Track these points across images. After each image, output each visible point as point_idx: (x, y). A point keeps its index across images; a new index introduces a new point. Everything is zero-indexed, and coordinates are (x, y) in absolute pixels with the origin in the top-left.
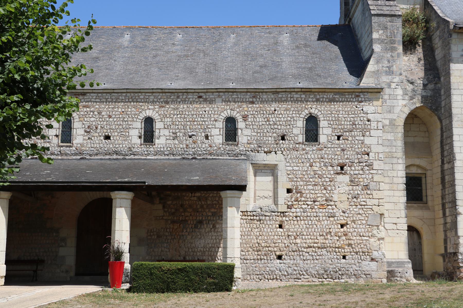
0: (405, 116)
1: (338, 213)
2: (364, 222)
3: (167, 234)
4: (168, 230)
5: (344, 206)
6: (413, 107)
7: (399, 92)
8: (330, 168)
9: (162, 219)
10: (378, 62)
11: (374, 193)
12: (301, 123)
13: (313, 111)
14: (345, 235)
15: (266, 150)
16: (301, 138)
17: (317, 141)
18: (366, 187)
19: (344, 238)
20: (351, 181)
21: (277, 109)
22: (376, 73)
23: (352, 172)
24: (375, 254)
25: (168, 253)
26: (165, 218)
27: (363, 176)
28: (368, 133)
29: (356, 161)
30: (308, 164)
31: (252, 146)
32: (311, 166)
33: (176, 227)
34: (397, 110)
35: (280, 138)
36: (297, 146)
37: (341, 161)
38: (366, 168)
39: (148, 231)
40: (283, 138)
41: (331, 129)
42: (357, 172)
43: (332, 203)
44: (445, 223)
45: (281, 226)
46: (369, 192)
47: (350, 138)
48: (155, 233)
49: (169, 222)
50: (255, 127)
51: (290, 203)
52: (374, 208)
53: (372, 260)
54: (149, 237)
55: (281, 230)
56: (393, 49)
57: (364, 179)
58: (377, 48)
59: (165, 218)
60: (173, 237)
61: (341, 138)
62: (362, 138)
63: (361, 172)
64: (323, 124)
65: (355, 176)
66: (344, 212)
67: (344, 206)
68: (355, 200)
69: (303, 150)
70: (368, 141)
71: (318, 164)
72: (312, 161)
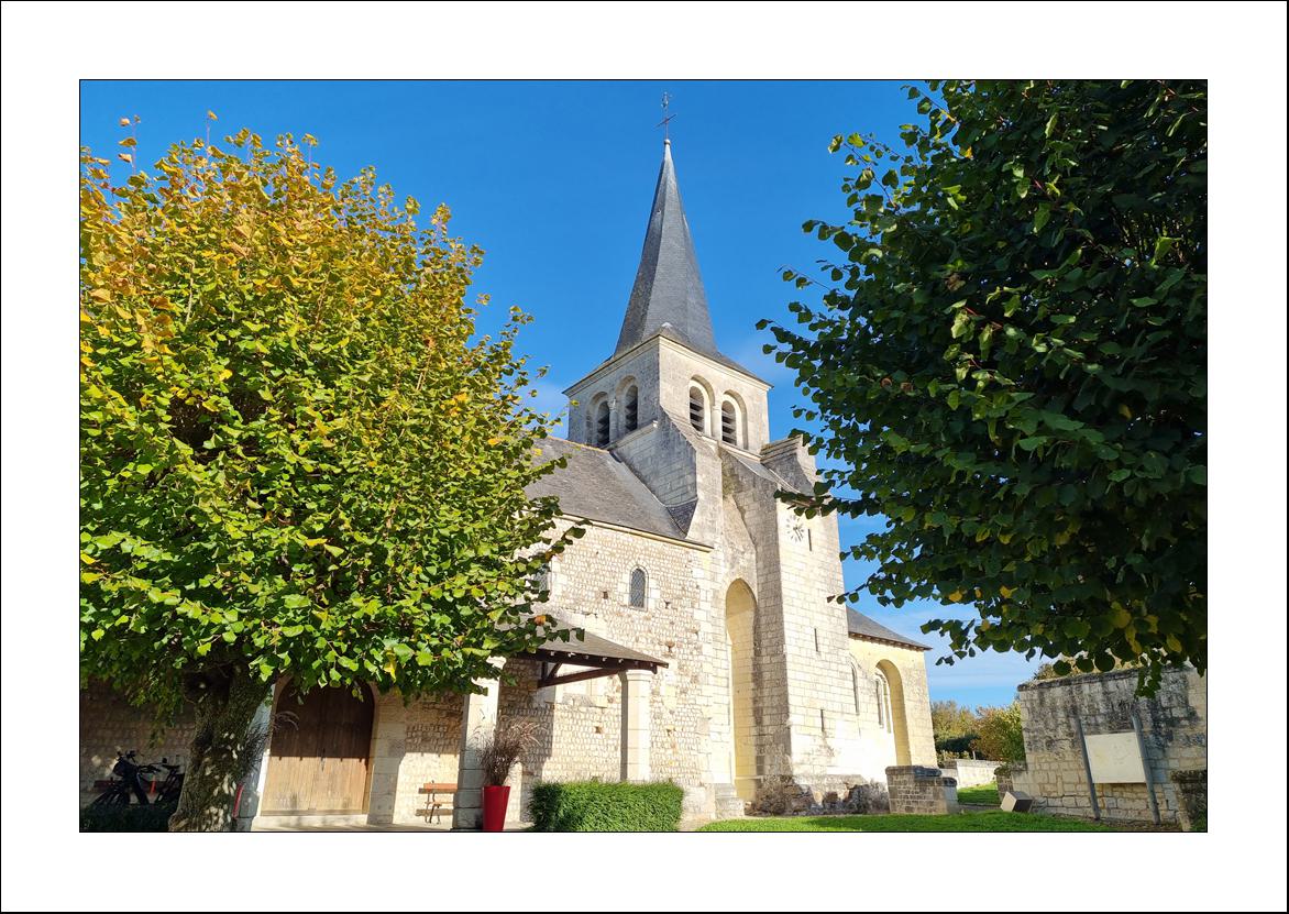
0: (726, 588)
1: (667, 715)
2: (692, 729)
3: (438, 735)
4: (441, 729)
5: (671, 703)
6: (734, 579)
7: (721, 556)
8: (657, 647)
9: (434, 708)
10: (702, 513)
11: (704, 687)
12: (627, 578)
13: (640, 562)
14: (673, 747)
15: (585, 609)
16: (626, 600)
17: (643, 606)
18: (695, 679)
19: (670, 752)
20: (680, 668)
21: (600, 552)
22: (701, 526)
23: (680, 657)
24: (704, 778)
25: (438, 771)
26: (438, 706)
27: (692, 663)
28: (696, 606)
29: (686, 641)
30: (634, 639)
31: (568, 601)
32: (637, 641)
33: (453, 724)
34: (720, 578)
35: (602, 595)
36: (622, 609)
37: (669, 639)
38: (695, 652)
39: (408, 728)
40: (606, 596)
41: (659, 592)
42: (686, 657)
43: (659, 699)
44: (760, 735)
45: (598, 730)
46: (698, 687)
47: (679, 609)
48: (420, 733)
49: (444, 713)
50: (572, 573)
51: (611, 695)
52: (704, 710)
53: (701, 785)
54: (410, 741)
55: (598, 735)
56: (715, 501)
57: (692, 667)
58: (701, 495)
59: (438, 706)
60: (447, 742)
61: (669, 606)
62: (691, 610)
63: (690, 657)
64: (651, 583)
65: (684, 663)
66: (672, 712)
67: (671, 703)
68: (683, 696)
69: (629, 616)
70: (698, 615)
71: (644, 640)
72: (638, 634)
